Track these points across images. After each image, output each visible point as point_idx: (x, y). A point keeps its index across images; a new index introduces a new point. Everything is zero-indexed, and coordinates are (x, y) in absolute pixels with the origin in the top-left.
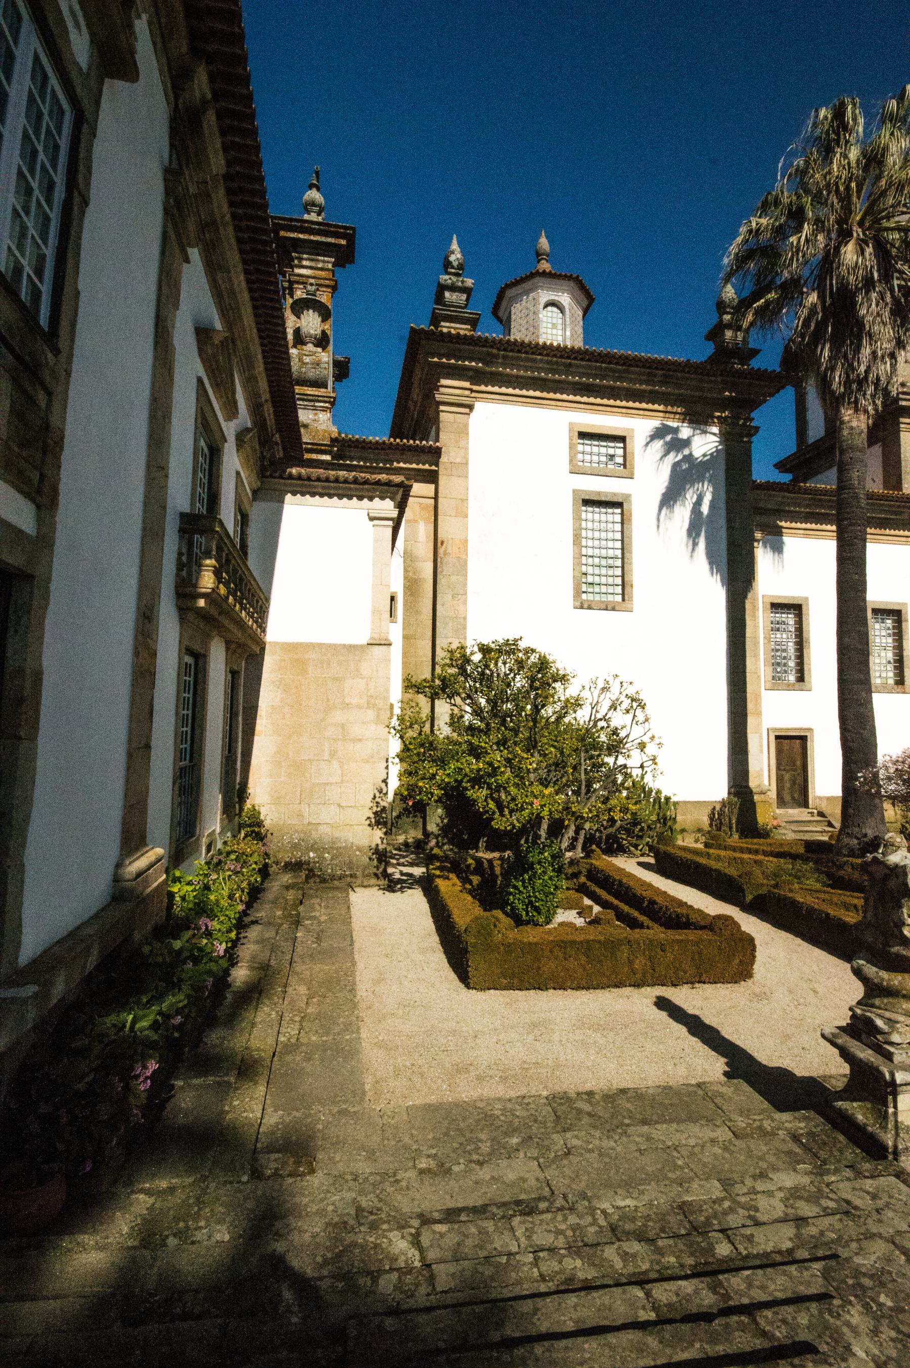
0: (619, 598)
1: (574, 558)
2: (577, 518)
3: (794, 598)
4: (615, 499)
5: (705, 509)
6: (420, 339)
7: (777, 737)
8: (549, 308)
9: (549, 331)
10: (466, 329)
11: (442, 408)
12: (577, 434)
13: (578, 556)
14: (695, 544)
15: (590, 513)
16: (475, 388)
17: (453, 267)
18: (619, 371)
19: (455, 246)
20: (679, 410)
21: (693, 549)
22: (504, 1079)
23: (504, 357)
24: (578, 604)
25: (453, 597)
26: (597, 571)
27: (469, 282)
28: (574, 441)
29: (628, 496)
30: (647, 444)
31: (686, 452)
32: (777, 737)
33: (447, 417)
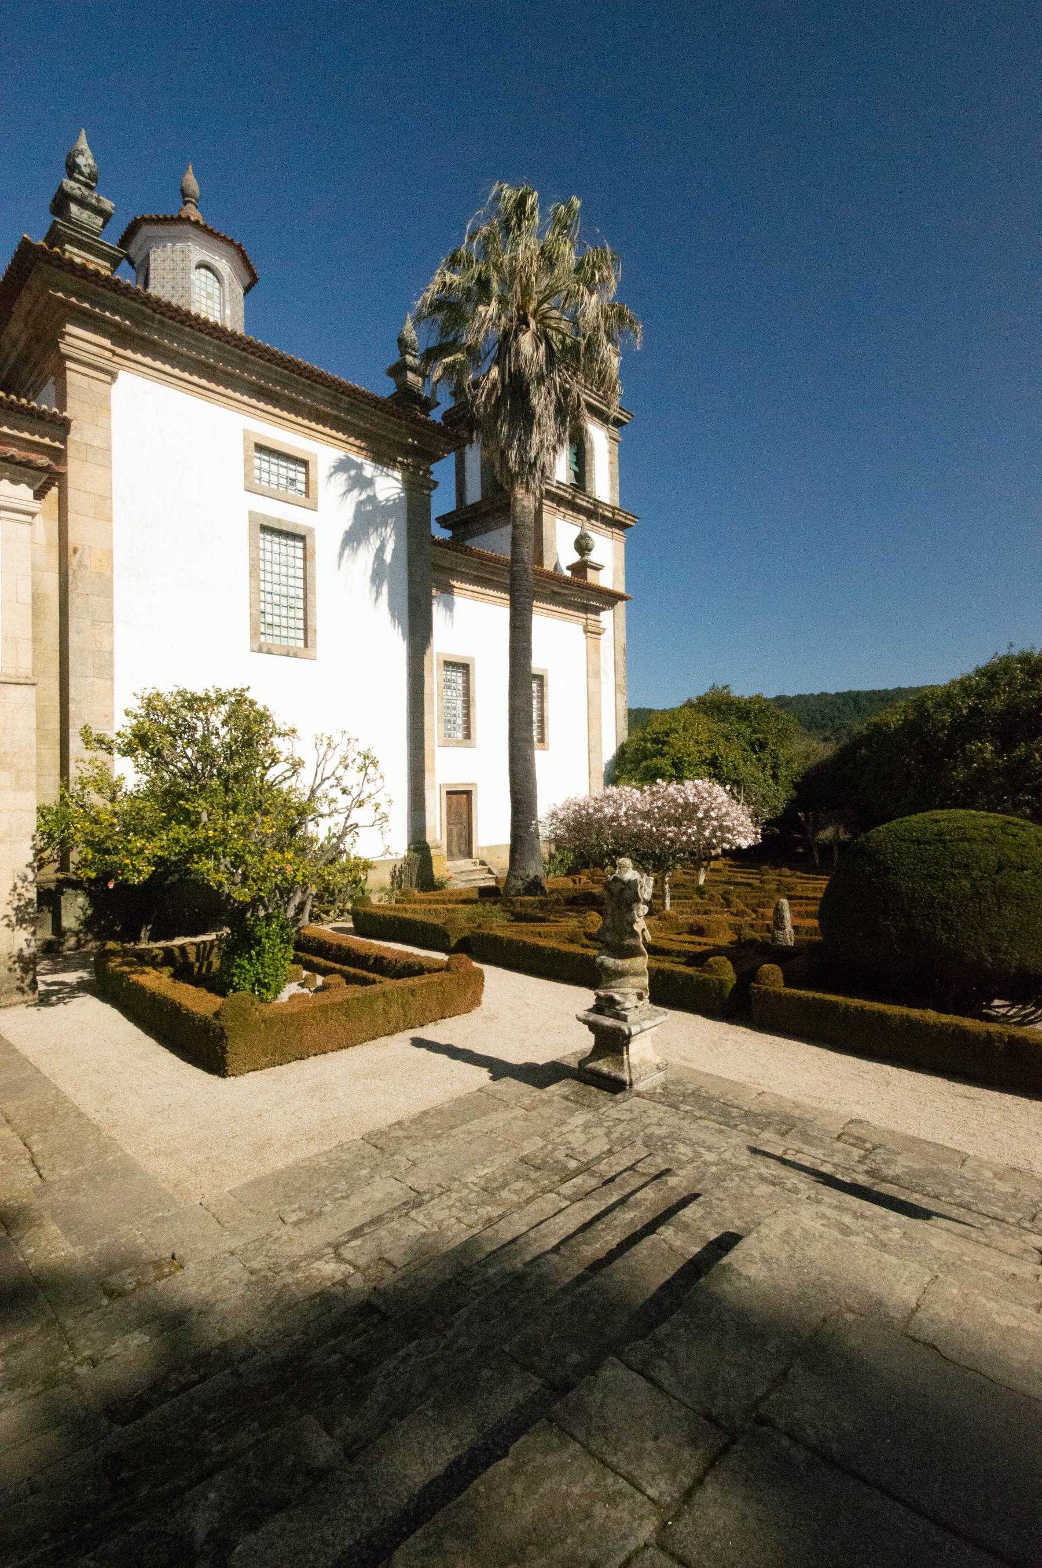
0: (301, 644)
2: (254, 546)
3: (463, 657)
4: (297, 531)
5: (388, 557)
6: (36, 259)
7: (449, 793)
8: (203, 271)
9: (203, 300)
10: (105, 267)
11: (69, 364)
12: (253, 445)
13: (256, 591)
14: (378, 593)
15: (269, 543)
16: (119, 351)
17: (81, 173)
18: (304, 384)
19: (83, 144)
20: (363, 445)
21: (376, 599)
22: (310, 1140)
23: (161, 322)
24: (256, 647)
25: (93, 624)
26: (276, 611)
27: (108, 205)
28: (250, 453)
30: (331, 475)
31: (369, 492)
32: (449, 793)
33: (76, 378)
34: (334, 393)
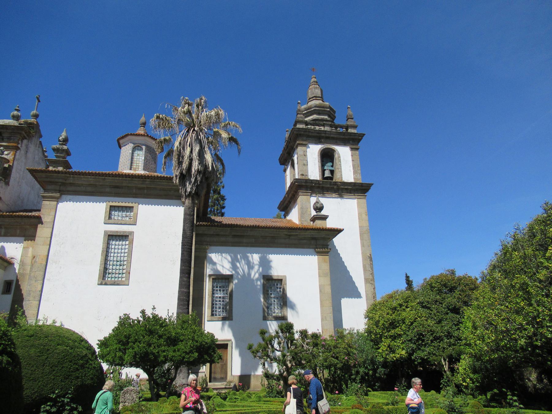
1: (101, 261)
4: (125, 234)
18: (129, 180)
23: (73, 177)
24: (100, 282)
29: (132, 233)
34: (142, 179)
